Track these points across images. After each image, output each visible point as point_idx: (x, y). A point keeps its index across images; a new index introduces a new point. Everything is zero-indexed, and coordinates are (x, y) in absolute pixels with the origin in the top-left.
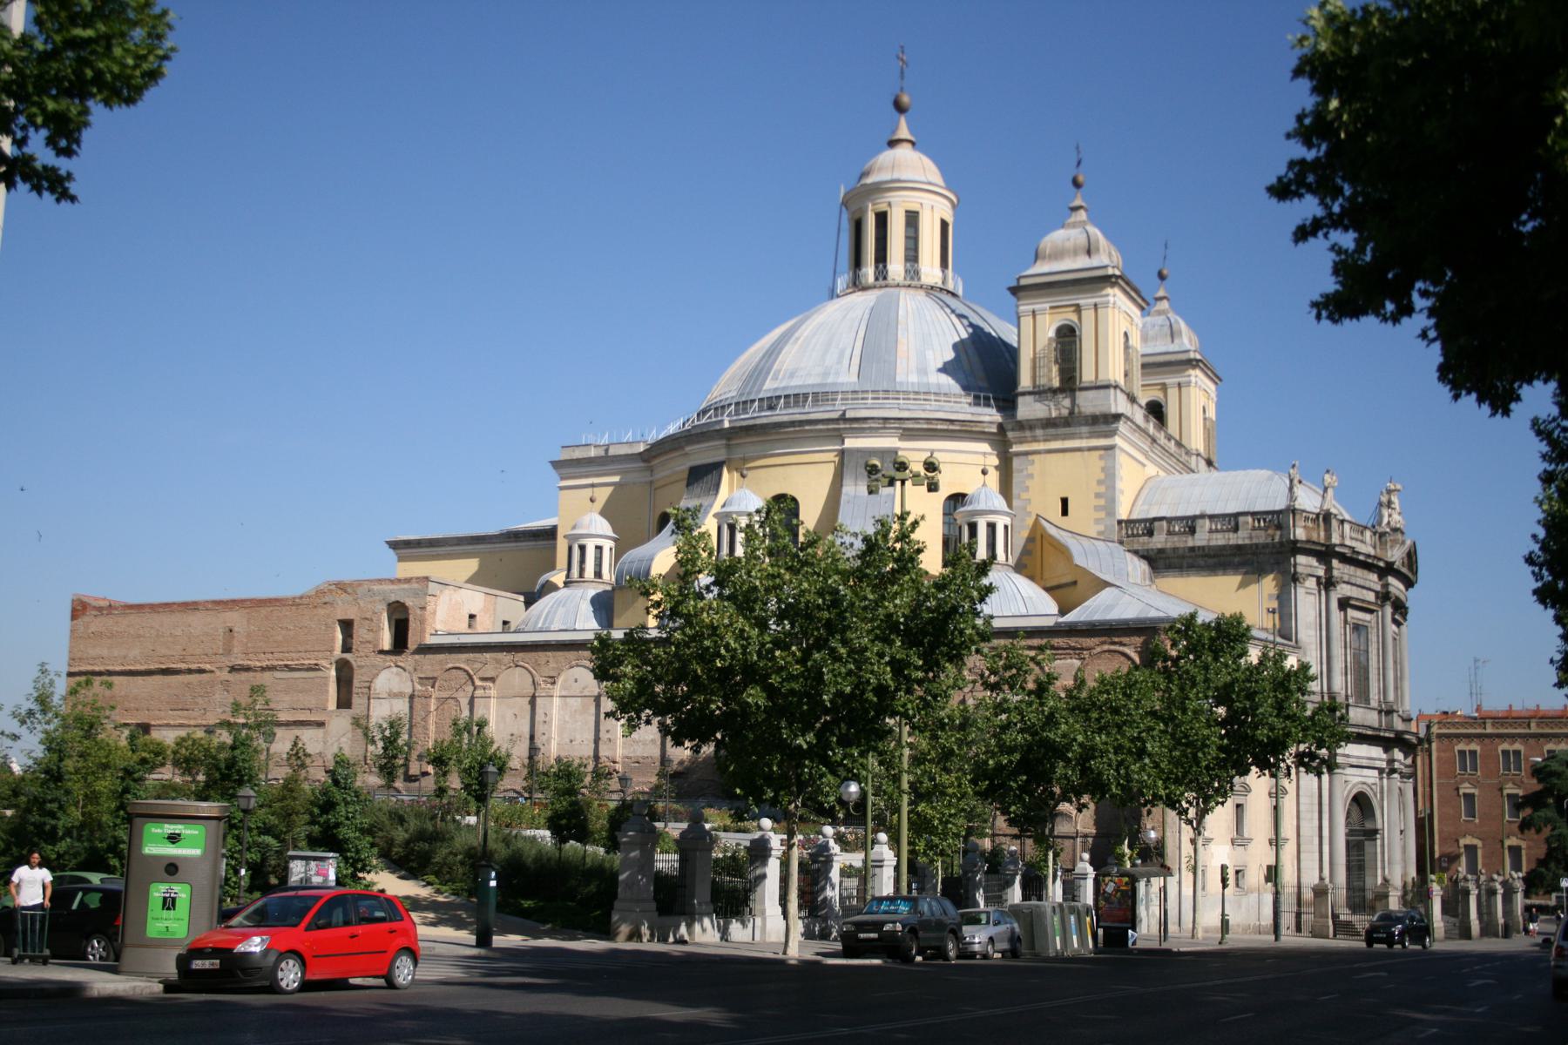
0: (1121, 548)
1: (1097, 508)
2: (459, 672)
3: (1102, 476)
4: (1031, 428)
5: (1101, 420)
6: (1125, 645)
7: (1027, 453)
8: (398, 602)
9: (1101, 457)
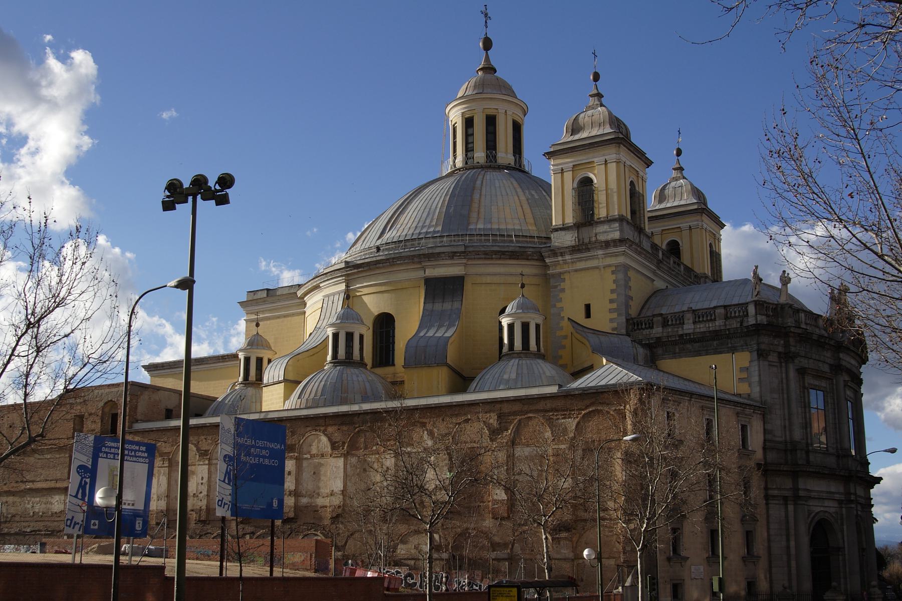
0: (628, 339)
1: (611, 311)
3: (614, 286)
4: (562, 254)
5: (612, 244)
7: (560, 273)
9: (613, 273)
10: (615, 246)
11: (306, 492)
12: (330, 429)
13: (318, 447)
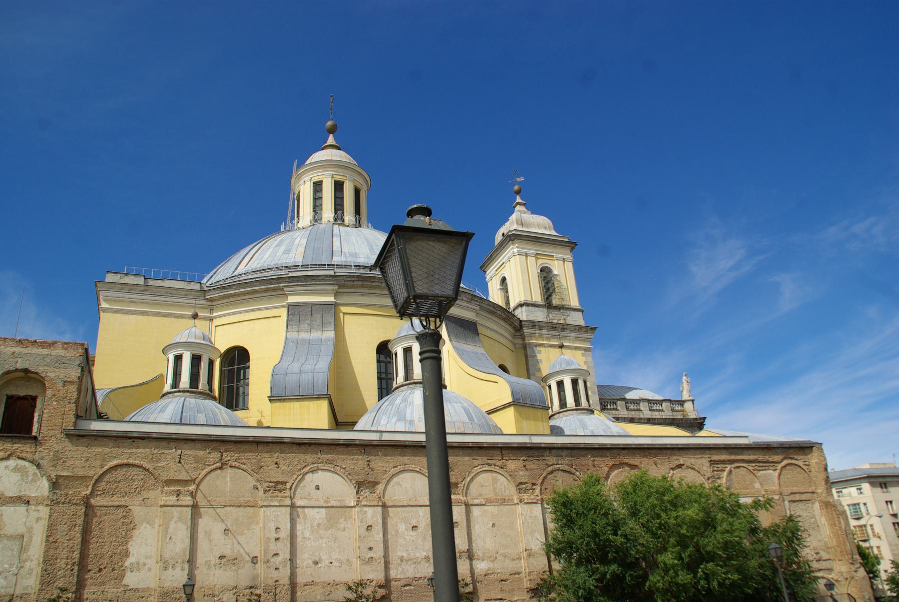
2: (133, 472)
4: (540, 328)
5: (584, 330)
6: (796, 459)
8: (26, 371)
9: (583, 355)
10: (586, 332)
11: (484, 554)
12: (512, 465)
13: (495, 488)
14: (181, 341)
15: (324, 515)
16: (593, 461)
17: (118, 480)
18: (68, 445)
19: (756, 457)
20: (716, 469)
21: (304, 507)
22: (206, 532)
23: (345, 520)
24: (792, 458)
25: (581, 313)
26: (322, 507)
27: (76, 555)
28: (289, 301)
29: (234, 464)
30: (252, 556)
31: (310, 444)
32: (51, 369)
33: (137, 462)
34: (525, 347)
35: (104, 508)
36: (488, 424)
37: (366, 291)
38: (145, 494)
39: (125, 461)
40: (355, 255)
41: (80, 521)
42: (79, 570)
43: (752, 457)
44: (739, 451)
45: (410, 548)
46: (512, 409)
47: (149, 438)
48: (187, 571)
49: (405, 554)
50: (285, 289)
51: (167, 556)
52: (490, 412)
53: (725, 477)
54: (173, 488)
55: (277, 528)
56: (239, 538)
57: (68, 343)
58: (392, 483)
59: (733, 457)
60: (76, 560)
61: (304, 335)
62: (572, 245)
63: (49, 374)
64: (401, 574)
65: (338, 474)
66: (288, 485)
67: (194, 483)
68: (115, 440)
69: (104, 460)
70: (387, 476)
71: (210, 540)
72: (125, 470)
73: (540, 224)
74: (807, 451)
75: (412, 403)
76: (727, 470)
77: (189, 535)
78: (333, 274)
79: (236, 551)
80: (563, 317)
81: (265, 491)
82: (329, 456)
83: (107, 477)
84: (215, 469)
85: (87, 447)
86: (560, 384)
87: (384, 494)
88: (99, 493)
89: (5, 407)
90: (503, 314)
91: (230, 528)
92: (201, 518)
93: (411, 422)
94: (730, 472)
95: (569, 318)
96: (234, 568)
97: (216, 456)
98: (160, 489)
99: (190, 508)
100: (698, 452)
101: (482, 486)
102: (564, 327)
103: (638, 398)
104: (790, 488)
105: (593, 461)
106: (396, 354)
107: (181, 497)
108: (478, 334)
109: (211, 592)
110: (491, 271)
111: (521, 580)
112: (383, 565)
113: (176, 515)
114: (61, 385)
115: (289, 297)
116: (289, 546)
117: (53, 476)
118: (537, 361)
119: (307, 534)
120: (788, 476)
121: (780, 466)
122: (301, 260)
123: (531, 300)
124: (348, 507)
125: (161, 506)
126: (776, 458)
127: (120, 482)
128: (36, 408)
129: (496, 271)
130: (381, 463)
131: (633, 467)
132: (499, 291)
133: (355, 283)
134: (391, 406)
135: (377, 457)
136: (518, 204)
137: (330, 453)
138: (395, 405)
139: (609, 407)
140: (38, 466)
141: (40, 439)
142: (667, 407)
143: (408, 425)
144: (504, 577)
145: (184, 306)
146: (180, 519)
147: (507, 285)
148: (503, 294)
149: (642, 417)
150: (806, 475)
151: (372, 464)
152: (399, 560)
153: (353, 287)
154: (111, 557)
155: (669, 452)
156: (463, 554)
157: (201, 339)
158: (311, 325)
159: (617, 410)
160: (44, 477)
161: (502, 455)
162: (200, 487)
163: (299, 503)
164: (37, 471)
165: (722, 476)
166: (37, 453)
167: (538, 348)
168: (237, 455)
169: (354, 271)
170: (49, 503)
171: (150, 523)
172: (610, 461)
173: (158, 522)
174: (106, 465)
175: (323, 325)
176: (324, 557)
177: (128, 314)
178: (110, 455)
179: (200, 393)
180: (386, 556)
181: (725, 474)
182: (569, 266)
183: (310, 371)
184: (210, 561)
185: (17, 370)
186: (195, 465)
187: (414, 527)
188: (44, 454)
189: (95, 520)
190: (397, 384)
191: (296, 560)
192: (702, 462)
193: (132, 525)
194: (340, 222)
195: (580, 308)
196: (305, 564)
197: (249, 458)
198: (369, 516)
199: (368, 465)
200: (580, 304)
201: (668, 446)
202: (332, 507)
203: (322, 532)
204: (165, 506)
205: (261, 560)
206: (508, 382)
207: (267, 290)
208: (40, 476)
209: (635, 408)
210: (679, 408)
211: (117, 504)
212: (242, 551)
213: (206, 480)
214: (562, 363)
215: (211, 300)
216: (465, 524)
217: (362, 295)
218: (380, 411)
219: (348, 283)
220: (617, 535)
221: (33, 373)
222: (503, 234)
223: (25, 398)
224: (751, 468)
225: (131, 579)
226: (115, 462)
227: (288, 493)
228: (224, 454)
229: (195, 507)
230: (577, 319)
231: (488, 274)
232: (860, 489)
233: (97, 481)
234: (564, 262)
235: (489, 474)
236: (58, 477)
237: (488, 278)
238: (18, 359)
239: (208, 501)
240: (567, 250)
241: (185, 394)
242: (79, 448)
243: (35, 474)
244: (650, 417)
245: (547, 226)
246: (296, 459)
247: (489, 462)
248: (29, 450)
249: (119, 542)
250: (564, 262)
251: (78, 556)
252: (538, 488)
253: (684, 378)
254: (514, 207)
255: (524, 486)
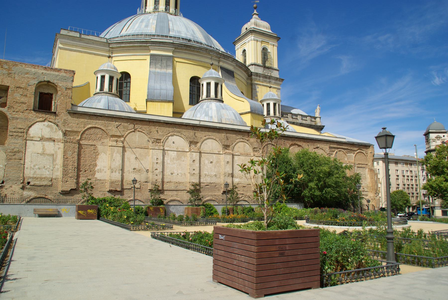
2: (98, 131)
4: (260, 77)
8: (49, 82)
10: (279, 81)
11: (238, 175)
13: (244, 149)
14: (104, 69)
15: (176, 154)
16: (284, 141)
17: (91, 134)
18: (69, 117)
19: (348, 147)
20: (331, 150)
21: (168, 150)
22: (128, 158)
23: (184, 157)
24: (361, 150)
25: (278, 72)
26: (175, 151)
27: (76, 164)
28: (151, 53)
29: (140, 130)
30: (146, 169)
31: (171, 124)
32: (59, 82)
33: (99, 126)
34: (252, 84)
35: (86, 146)
36: (242, 121)
37: (187, 52)
38: (103, 140)
39: (94, 126)
40: (179, 32)
41: (76, 150)
42: (77, 170)
43: (346, 147)
44: (342, 144)
45: (209, 171)
46: (250, 114)
47: (104, 116)
48: (121, 174)
49: (207, 173)
50: (149, 47)
51: (112, 167)
52: (241, 114)
53: (334, 154)
54: (114, 139)
55: (157, 159)
56: (142, 162)
57: (67, 70)
58: (203, 143)
59: (339, 146)
60: (76, 166)
61: (158, 70)
62: (278, 39)
63: (59, 84)
64: (205, 181)
65: (182, 138)
66: (162, 141)
67: (123, 137)
68: (89, 116)
69: (85, 124)
70: (202, 140)
71: (129, 161)
72: (94, 129)
73: (265, 26)
74: (368, 147)
75: (211, 109)
76: (336, 151)
77: (121, 159)
78: (172, 42)
79: (140, 167)
80: (270, 73)
81: (152, 142)
82: (179, 130)
83: (87, 132)
84: (132, 132)
85: (77, 118)
86: (268, 105)
87: (200, 147)
88: (83, 139)
89: (39, 98)
90: (245, 69)
91: (138, 157)
92: (126, 152)
93: (211, 117)
94: (337, 152)
95: (272, 73)
96: (139, 174)
97: (132, 126)
98: (109, 139)
99: (122, 148)
100: (325, 143)
101: (239, 148)
102: (270, 77)
103: (297, 113)
104: (358, 162)
105: (284, 141)
106: (203, 85)
107: (118, 143)
108: (234, 77)
109: (130, 183)
110: (238, 46)
111: (251, 187)
112: (199, 177)
113: (116, 150)
114: (65, 89)
115: (151, 51)
116: (162, 166)
117: (64, 130)
118: (256, 92)
119: (169, 162)
120: (359, 157)
121: (356, 152)
122: (154, 32)
123: (257, 62)
124: (185, 152)
125: (110, 146)
126: (355, 149)
127: (92, 134)
128: (52, 99)
129: (241, 46)
130: (200, 134)
131: (299, 146)
132: (241, 56)
133: (183, 48)
134: (202, 109)
135: (198, 132)
136: (255, 14)
137: (179, 128)
138: (203, 109)
139: (284, 116)
140: (57, 125)
141: (57, 113)
142: (309, 119)
143: (210, 119)
144: (245, 186)
145: (99, 50)
146: (118, 152)
147: (246, 53)
148: (243, 57)
149: (298, 122)
150: (365, 157)
151: (196, 134)
152: (205, 175)
153: (181, 49)
154: (90, 166)
155: (314, 141)
156: (230, 175)
157: (113, 69)
158: (161, 65)
159: (288, 118)
160: (60, 130)
161: (248, 135)
162: (126, 139)
163: (166, 149)
164: (57, 128)
165: (333, 153)
166: (56, 120)
167: (258, 86)
168: (141, 126)
169: (182, 42)
170: (63, 141)
171: (105, 153)
172: (291, 142)
173: (108, 152)
174: (86, 127)
175: (167, 66)
176: (175, 172)
177: (72, 51)
178: (87, 123)
179: (113, 94)
180: (200, 173)
181: (334, 153)
182: (275, 48)
183: (165, 89)
184: (130, 170)
185: (45, 81)
186: (123, 129)
187: (211, 162)
188: (59, 120)
189: (82, 150)
190: (202, 98)
191: (164, 172)
192: (326, 147)
193: (98, 153)
194: (168, 11)
195: (278, 69)
196: (167, 174)
197: (146, 128)
198: (194, 156)
199: (195, 135)
200: (278, 67)
201: (314, 139)
202: (179, 151)
203: (175, 161)
204: (111, 146)
205: (150, 171)
206: (249, 102)
207: (140, 46)
208: (58, 130)
209: (296, 118)
210: (314, 120)
211: (91, 144)
212: (142, 167)
213: (128, 136)
214: (270, 95)
215: (112, 48)
216: (232, 163)
217: (185, 54)
218: (196, 110)
219: (180, 47)
220: (294, 173)
221: (52, 83)
222: (246, 29)
223: (48, 94)
224: (345, 152)
225: (98, 176)
226: (90, 126)
227: (161, 144)
228: (135, 125)
229: (124, 147)
230: (276, 74)
231: (237, 47)
232: (378, 163)
233: (83, 134)
234: (273, 46)
235: (243, 143)
236: (66, 131)
237: (236, 48)
238: (45, 76)
239: (129, 145)
240: (276, 41)
241: (107, 94)
242: (74, 119)
243: (56, 129)
244: (301, 122)
245: (268, 27)
246: (165, 130)
247: (243, 138)
248: (53, 118)
249: (92, 160)
250: (273, 46)
251: (77, 165)
252: (261, 150)
253: (318, 107)
254: (253, 15)
255: (256, 149)
